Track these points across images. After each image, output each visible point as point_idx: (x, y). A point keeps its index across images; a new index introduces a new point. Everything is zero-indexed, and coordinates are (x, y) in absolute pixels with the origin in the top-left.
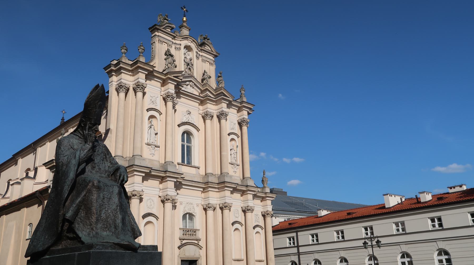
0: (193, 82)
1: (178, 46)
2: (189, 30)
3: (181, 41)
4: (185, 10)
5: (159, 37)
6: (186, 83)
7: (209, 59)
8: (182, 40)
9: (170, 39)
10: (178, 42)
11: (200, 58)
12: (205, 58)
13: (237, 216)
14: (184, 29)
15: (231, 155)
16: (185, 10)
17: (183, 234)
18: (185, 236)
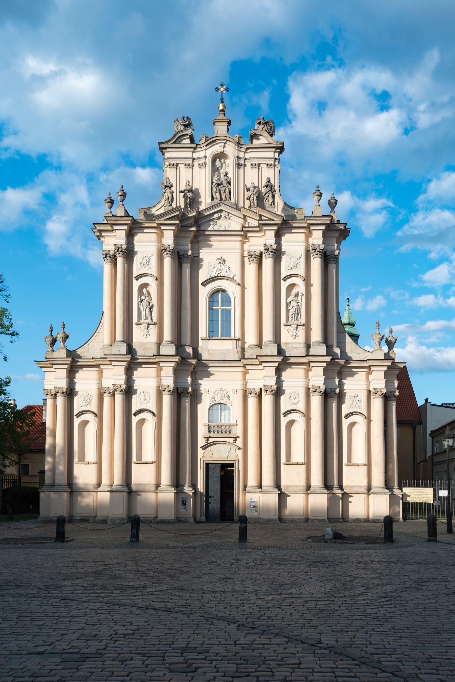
0: (226, 211)
1: (202, 161)
2: (229, 123)
3: (206, 149)
4: (222, 89)
5: (169, 159)
6: (214, 216)
7: (264, 160)
8: (207, 148)
9: (189, 154)
10: (202, 154)
11: (248, 164)
12: (256, 160)
13: (296, 401)
14: (217, 126)
15: (288, 311)
16: (222, 89)
17: (210, 432)
18: (212, 433)
